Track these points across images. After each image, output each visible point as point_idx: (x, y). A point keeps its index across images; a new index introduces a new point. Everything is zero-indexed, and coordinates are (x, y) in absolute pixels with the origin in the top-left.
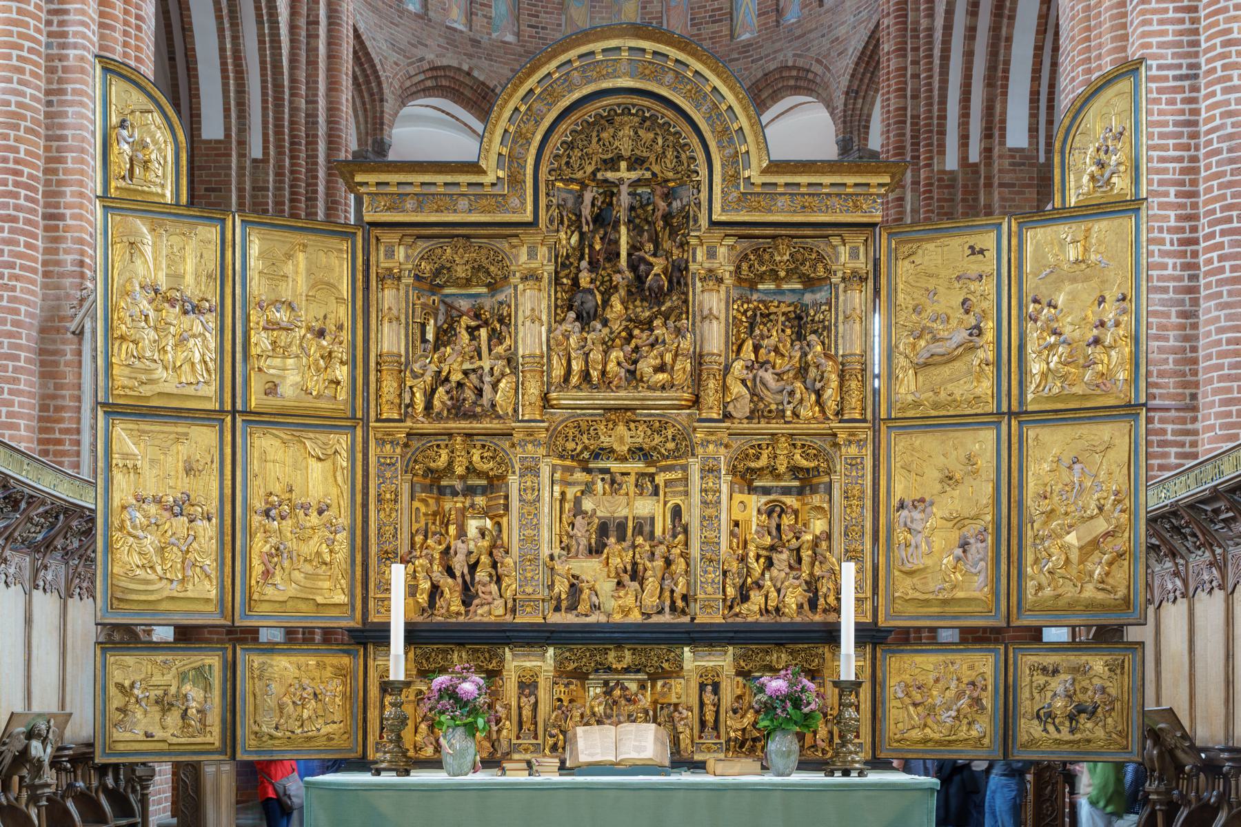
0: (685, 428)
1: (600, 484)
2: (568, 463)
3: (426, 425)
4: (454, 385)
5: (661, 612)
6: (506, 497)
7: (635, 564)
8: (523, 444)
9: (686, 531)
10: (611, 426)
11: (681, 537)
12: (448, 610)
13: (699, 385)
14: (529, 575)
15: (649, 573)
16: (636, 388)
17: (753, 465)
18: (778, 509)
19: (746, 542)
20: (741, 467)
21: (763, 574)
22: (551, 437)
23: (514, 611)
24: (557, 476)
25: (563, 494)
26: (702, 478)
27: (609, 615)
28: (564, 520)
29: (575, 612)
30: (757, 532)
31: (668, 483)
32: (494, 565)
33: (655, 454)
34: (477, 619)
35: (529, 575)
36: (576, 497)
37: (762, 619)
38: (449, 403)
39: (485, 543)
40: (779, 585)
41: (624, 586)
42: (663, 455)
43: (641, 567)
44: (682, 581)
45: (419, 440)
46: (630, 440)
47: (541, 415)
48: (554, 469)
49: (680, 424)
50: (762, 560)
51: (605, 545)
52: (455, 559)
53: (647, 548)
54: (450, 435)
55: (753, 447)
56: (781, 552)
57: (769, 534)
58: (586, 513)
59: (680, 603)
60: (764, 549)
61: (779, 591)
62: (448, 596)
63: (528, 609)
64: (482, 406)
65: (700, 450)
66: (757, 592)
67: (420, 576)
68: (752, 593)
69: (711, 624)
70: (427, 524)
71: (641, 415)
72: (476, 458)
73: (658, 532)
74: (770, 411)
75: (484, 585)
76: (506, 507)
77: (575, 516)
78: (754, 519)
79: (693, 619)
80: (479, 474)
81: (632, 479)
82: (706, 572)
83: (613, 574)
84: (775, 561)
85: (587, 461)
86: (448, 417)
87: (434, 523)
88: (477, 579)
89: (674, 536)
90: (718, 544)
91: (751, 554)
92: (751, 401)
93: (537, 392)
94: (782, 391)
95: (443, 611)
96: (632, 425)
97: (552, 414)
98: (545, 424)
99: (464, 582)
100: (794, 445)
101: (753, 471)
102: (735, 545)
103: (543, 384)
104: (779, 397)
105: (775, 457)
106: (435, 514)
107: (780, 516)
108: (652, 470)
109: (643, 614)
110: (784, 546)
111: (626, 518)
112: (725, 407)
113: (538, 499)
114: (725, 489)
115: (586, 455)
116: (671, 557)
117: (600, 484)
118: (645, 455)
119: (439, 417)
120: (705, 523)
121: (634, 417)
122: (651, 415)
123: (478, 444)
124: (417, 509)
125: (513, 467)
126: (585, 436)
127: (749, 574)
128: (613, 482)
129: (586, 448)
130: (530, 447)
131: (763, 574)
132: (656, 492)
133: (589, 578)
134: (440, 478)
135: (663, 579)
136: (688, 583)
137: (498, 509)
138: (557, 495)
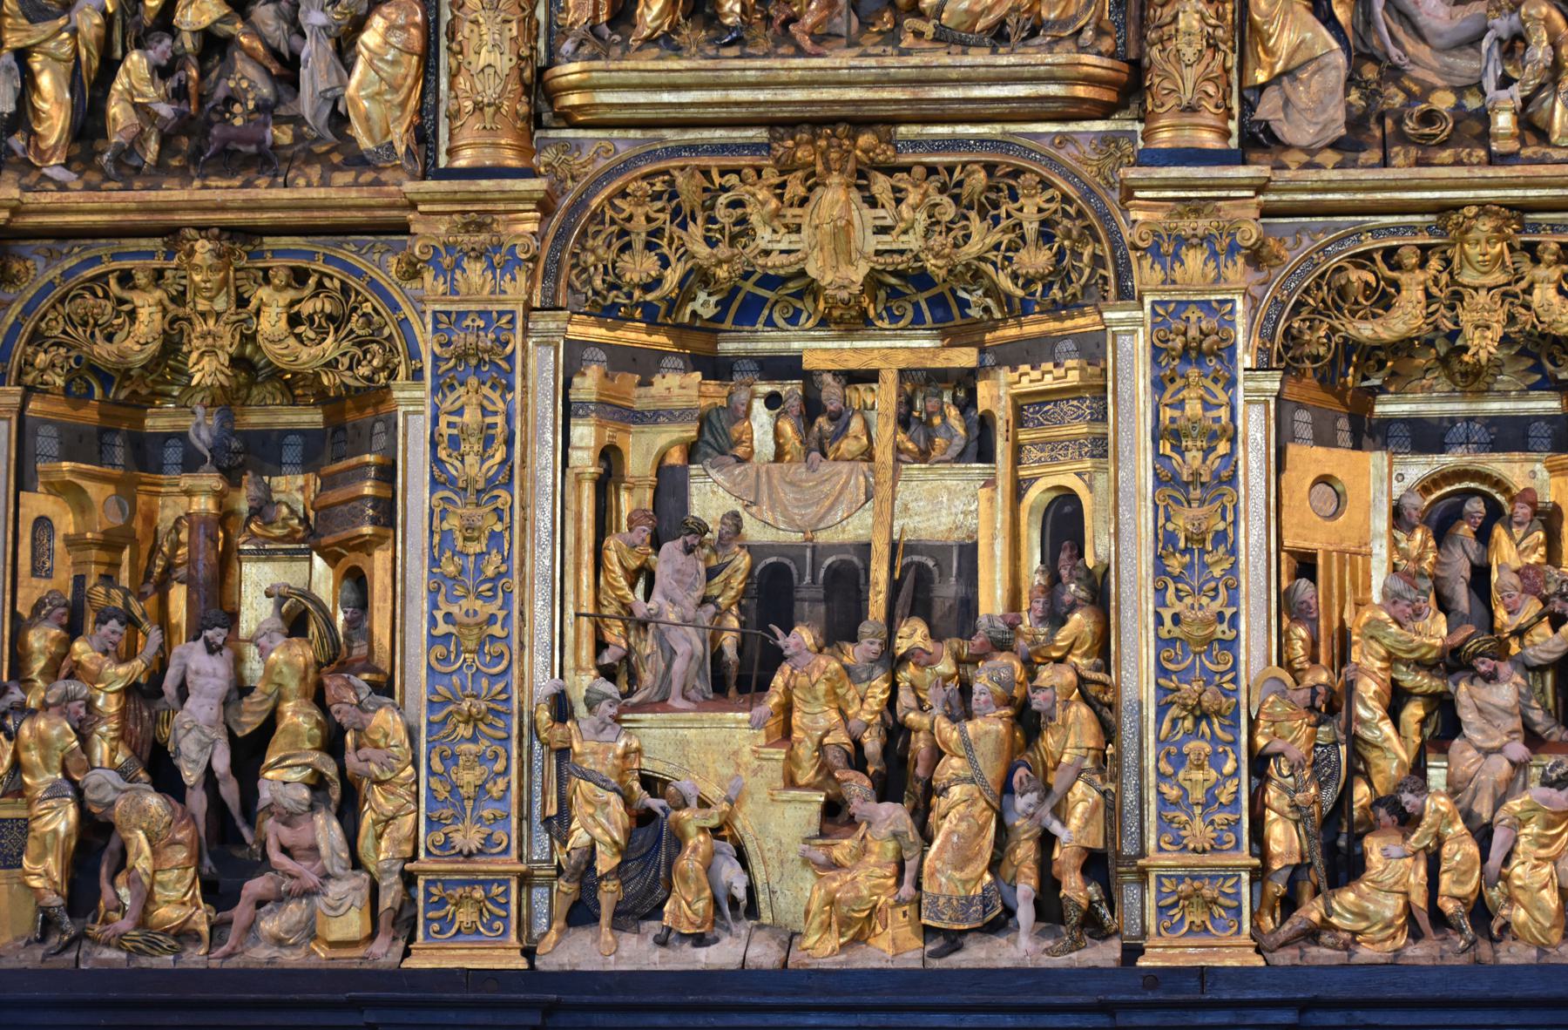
0: (1089, 193)
1: (761, 417)
2: (634, 336)
3: (74, 198)
4: (189, 43)
5: (1002, 923)
6: (387, 473)
7: (896, 732)
8: (447, 260)
9: (1099, 594)
10: (795, 188)
11: (1079, 622)
12: (142, 923)
13: (1143, 23)
14: (468, 778)
15: (952, 765)
16: (891, 37)
17: (1366, 331)
18: (1476, 506)
19: (1343, 640)
20: (1317, 339)
21: (1418, 769)
22: (562, 235)
23: (405, 924)
24: (587, 385)
25: (610, 456)
26: (1159, 385)
27: (791, 938)
28: (612, 556)
29: (653, 927)
30: (1392, 597)
31: (1026, 408)
32: (333, 742)
33: (975, 297)
34: (261, 954)
35: (468, 778)
36: (661, 469)
37: (1419, 953)
38: (165, 110)
39: (299, 654)
40: (1483, 809)
41: (852, 823)
42: (1006, 300)
43: (920, 744)
44: (1082, 797)
45: (51, 257)
46: (873, 243)
47: (527, 148)
48: (575, 357)
49: (1070, 174)
50: (1414, 712)
51: (775, 658)
52: (182, 718)
53: (946, 666)
54: (171, 234)
55: (1363, 260)
56: (1491, 678)
57: (1444, 605)
58: (701, 528)
59: (1075, 888)
60: (1420, 665)
61: (1483, 835)
62: (142, 862)
63: (465, 916)
64: (297, 120)
65: (1146, 274)
66: (1395, 845)
67: (40, 781)
68: (1374, 847)
69: (1202, 973)
70: (79, 581)
71: (915, 144)
72: (271, 322)
73: (992, 600)
74: (1429, 118)
75: (288, 819)
76: (386, 512)
77: (656, 544)
78: (1380, 552)
79: (1132, 952)
80: (293, 386)
81: (884, 397)
82: (1179, 760)
83: (806, 774)
84: (1467, 715)
85: (711, 329)
86: (161, 166)
87: (108, 579)
88: (265, 795)
89: (1055, 617)
90: (1231, 645)
91: (1369, 688)
92: (1351, 81)
93: (505, 63)
94: (1474, 41)
95: (123, 924)
96: (881, 185)
97: (567, 146)
98: (538, 185)
99: (217, 804)
100: (1530, 248)
101: (1371, 355)
102: (1299, 649)
103: (529, 28)
104: (1464, 64)
105: (1457, 297)
106: (111, 543)
107: (1483, 536)
108: (965, 358)
109: (928, 932)
110: (1501, 651)
111: (864, 549)
112: (1248, 106)
113: (505, 476)
114: (1255, 427)
115: (704, 304)
116: (1038, 701)
117: (761, 417)
118: (938, 303)
119: (127, 166)
120: (1175, 564)
121: (885, 154)
122: (955, 144)
123: (280, 268)
124: (43, 523)
125: (414, 354)
126: (696, 230)
127: (1359, 767)
128: (812, 407)
129: (700, 277)
130: (475, 272)
131: (1418, 769)
132: (985, 453)
133: (713, 791)
134: (139, 404)
135: (1007, 788)
136: (1111, 809)
137: (355, 519)
138: (584, 459)
